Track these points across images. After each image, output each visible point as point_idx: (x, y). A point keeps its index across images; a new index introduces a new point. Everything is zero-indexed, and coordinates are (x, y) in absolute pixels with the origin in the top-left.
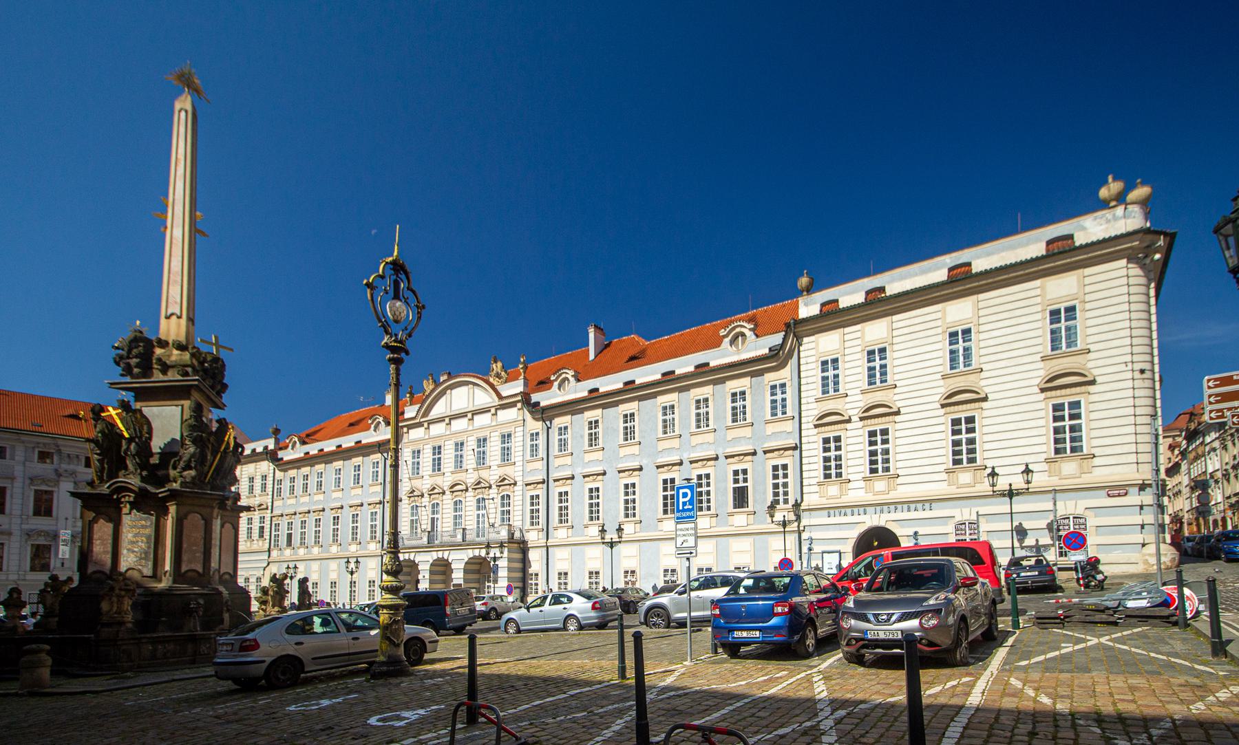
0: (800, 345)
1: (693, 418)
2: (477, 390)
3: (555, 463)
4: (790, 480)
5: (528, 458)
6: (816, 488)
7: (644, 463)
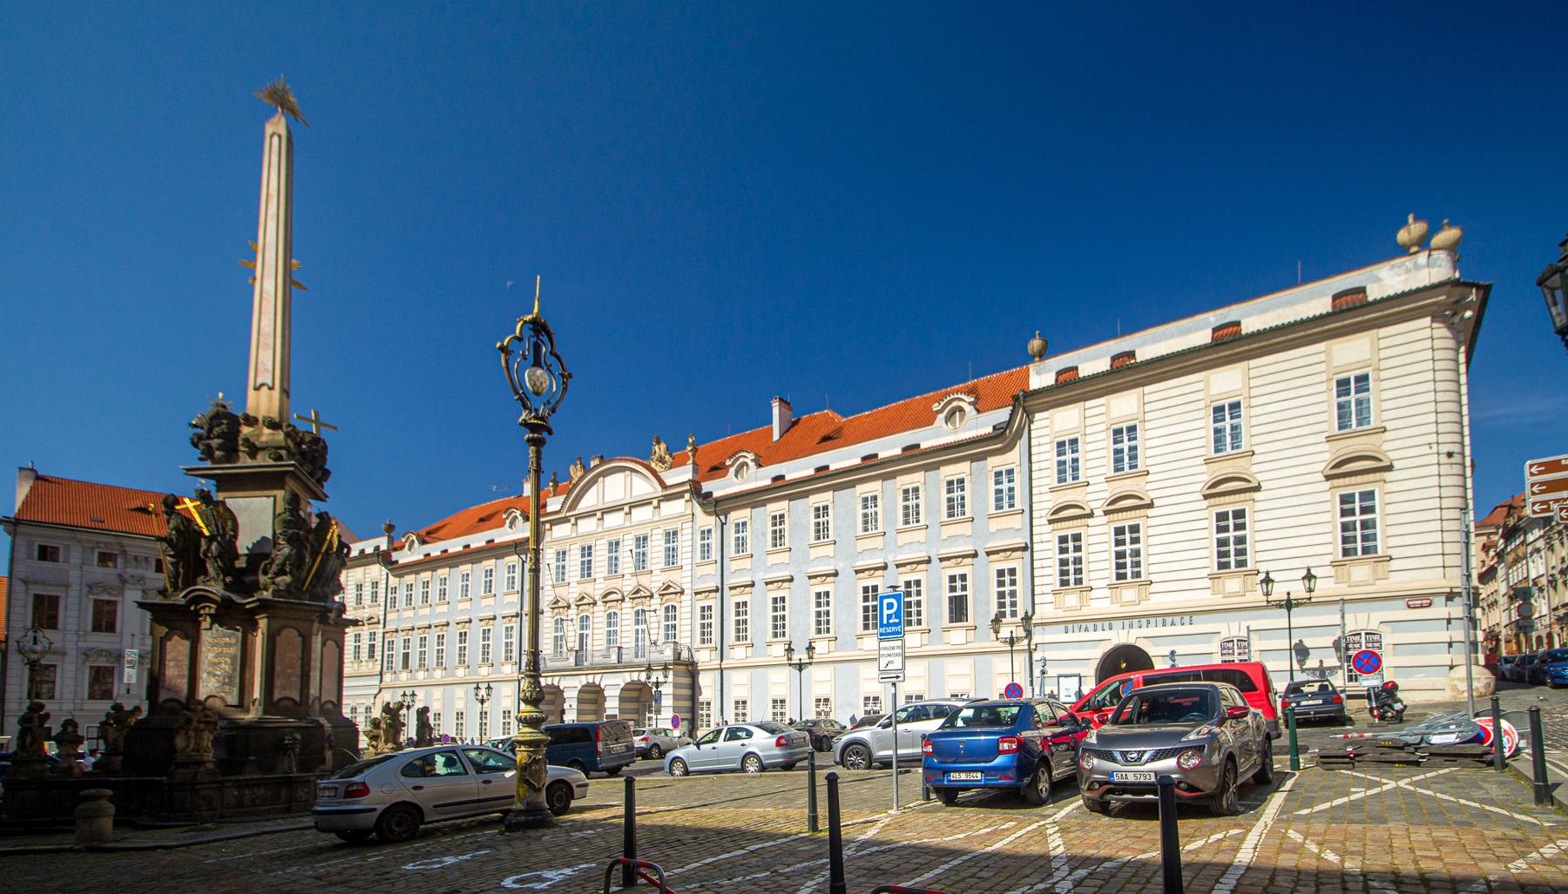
0: (1031, 422)
1: (900, 512)
2: (636, 478)
3: (731, 566)
4: (1018, 587)
5: (698, 559)
6: (1050, 598)
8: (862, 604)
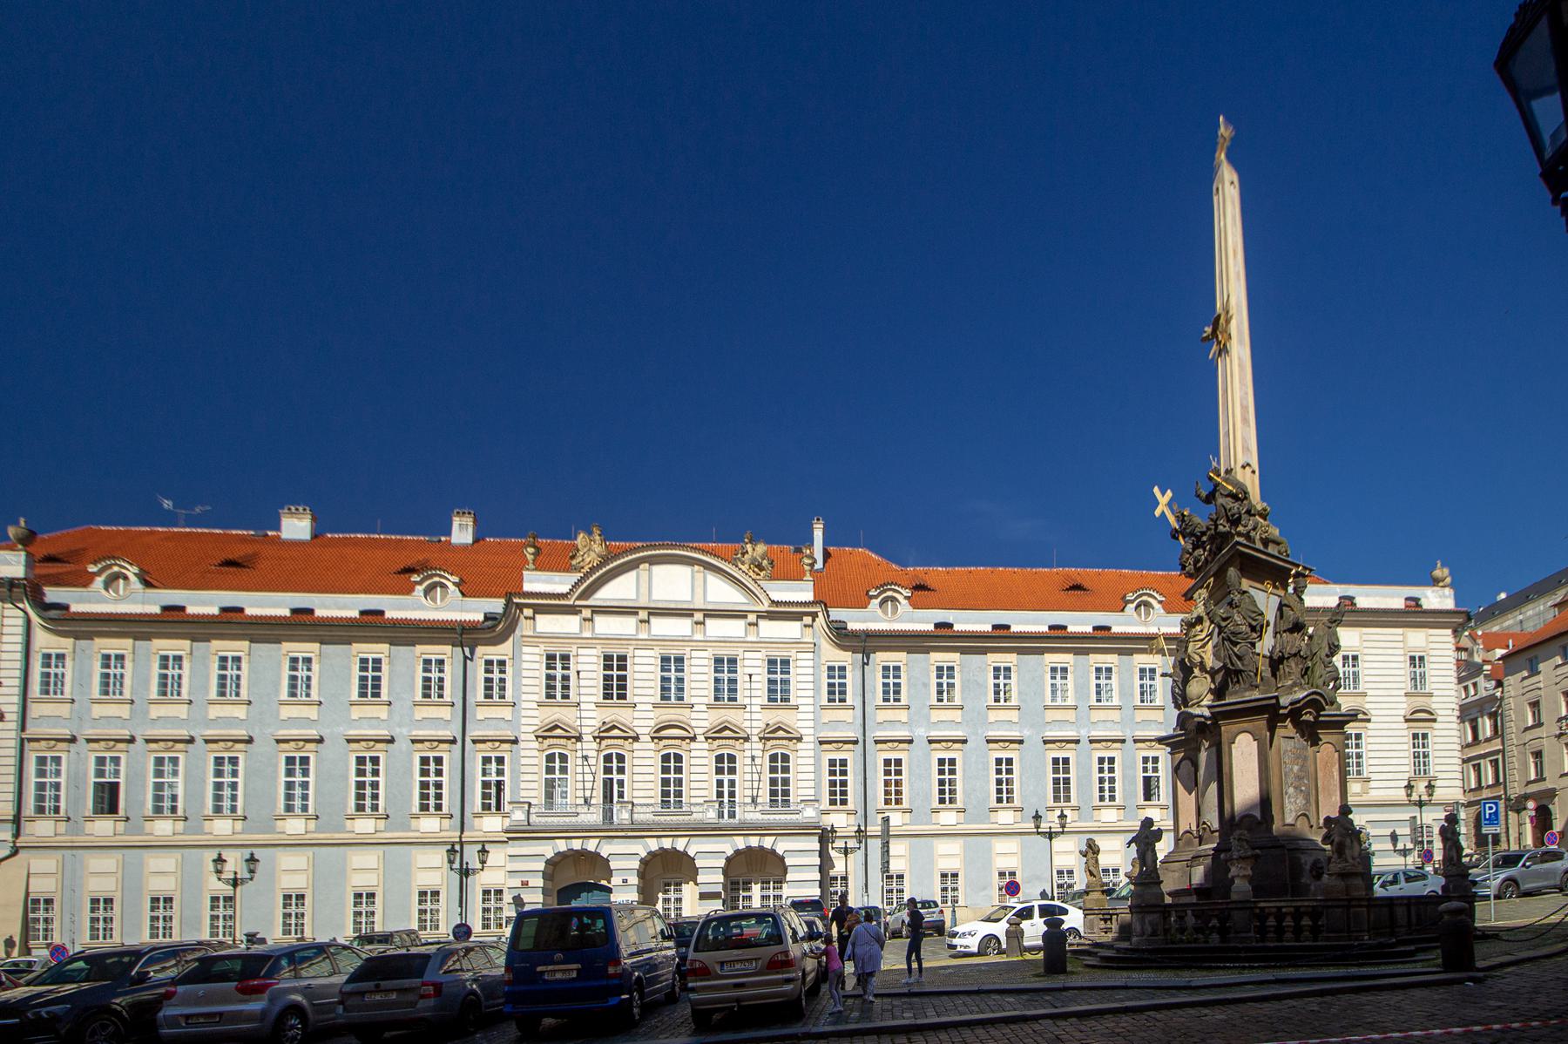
7: (1026, 733)
8: (1051, 776)
